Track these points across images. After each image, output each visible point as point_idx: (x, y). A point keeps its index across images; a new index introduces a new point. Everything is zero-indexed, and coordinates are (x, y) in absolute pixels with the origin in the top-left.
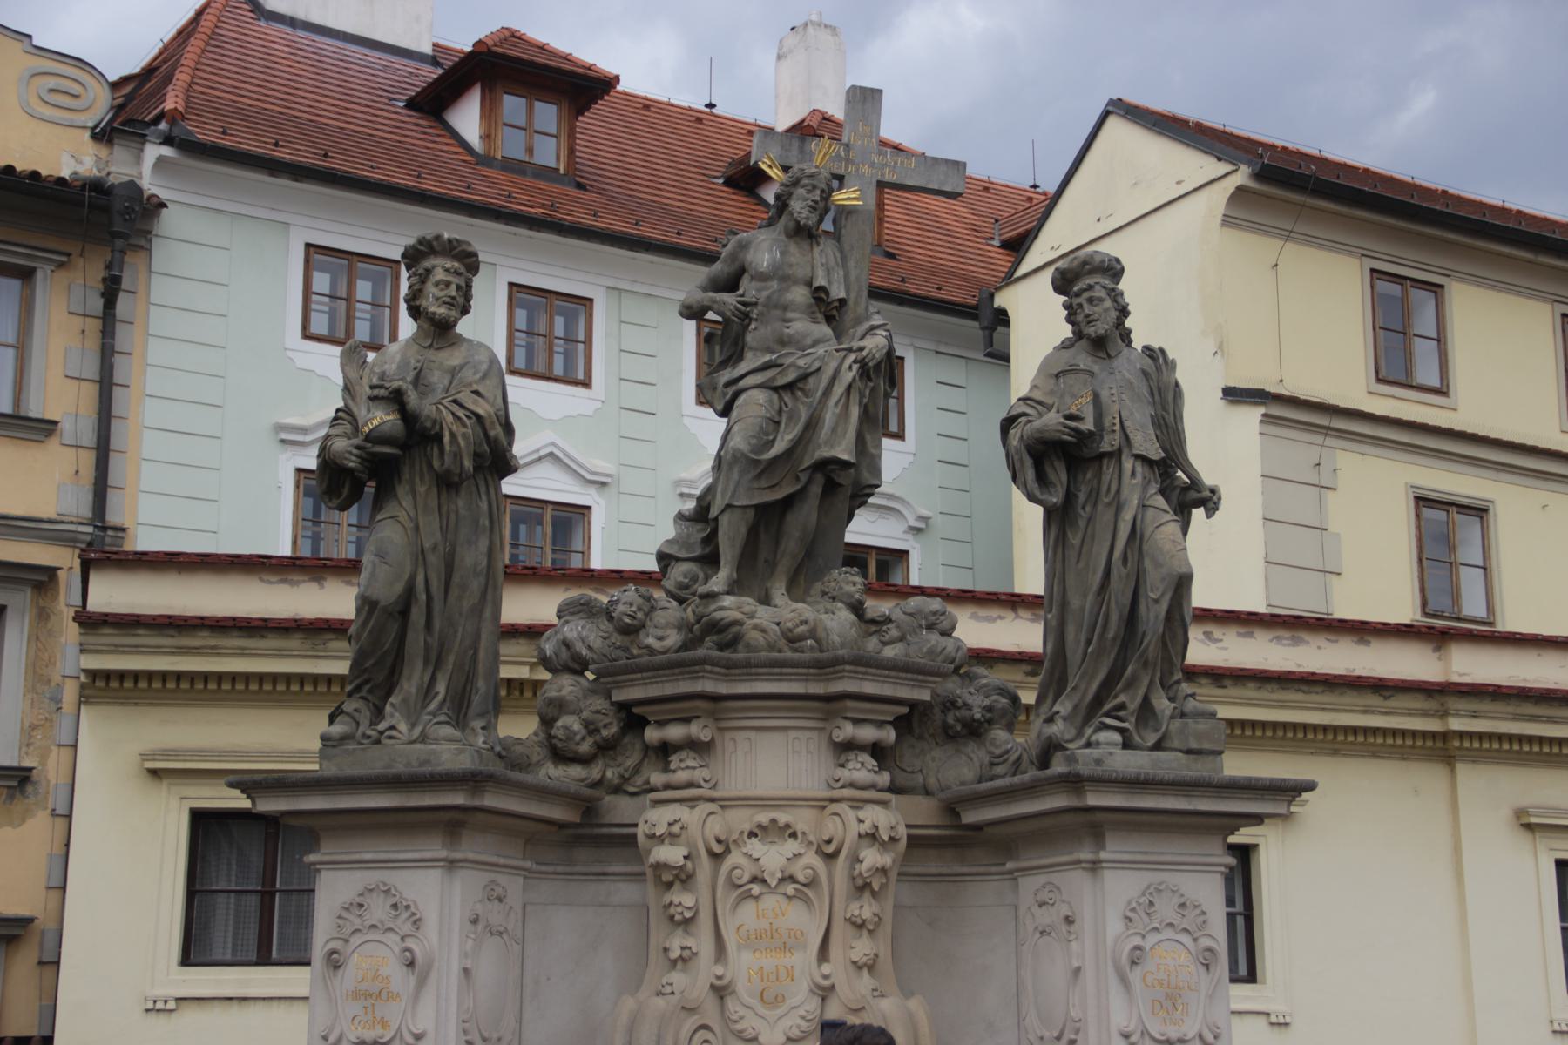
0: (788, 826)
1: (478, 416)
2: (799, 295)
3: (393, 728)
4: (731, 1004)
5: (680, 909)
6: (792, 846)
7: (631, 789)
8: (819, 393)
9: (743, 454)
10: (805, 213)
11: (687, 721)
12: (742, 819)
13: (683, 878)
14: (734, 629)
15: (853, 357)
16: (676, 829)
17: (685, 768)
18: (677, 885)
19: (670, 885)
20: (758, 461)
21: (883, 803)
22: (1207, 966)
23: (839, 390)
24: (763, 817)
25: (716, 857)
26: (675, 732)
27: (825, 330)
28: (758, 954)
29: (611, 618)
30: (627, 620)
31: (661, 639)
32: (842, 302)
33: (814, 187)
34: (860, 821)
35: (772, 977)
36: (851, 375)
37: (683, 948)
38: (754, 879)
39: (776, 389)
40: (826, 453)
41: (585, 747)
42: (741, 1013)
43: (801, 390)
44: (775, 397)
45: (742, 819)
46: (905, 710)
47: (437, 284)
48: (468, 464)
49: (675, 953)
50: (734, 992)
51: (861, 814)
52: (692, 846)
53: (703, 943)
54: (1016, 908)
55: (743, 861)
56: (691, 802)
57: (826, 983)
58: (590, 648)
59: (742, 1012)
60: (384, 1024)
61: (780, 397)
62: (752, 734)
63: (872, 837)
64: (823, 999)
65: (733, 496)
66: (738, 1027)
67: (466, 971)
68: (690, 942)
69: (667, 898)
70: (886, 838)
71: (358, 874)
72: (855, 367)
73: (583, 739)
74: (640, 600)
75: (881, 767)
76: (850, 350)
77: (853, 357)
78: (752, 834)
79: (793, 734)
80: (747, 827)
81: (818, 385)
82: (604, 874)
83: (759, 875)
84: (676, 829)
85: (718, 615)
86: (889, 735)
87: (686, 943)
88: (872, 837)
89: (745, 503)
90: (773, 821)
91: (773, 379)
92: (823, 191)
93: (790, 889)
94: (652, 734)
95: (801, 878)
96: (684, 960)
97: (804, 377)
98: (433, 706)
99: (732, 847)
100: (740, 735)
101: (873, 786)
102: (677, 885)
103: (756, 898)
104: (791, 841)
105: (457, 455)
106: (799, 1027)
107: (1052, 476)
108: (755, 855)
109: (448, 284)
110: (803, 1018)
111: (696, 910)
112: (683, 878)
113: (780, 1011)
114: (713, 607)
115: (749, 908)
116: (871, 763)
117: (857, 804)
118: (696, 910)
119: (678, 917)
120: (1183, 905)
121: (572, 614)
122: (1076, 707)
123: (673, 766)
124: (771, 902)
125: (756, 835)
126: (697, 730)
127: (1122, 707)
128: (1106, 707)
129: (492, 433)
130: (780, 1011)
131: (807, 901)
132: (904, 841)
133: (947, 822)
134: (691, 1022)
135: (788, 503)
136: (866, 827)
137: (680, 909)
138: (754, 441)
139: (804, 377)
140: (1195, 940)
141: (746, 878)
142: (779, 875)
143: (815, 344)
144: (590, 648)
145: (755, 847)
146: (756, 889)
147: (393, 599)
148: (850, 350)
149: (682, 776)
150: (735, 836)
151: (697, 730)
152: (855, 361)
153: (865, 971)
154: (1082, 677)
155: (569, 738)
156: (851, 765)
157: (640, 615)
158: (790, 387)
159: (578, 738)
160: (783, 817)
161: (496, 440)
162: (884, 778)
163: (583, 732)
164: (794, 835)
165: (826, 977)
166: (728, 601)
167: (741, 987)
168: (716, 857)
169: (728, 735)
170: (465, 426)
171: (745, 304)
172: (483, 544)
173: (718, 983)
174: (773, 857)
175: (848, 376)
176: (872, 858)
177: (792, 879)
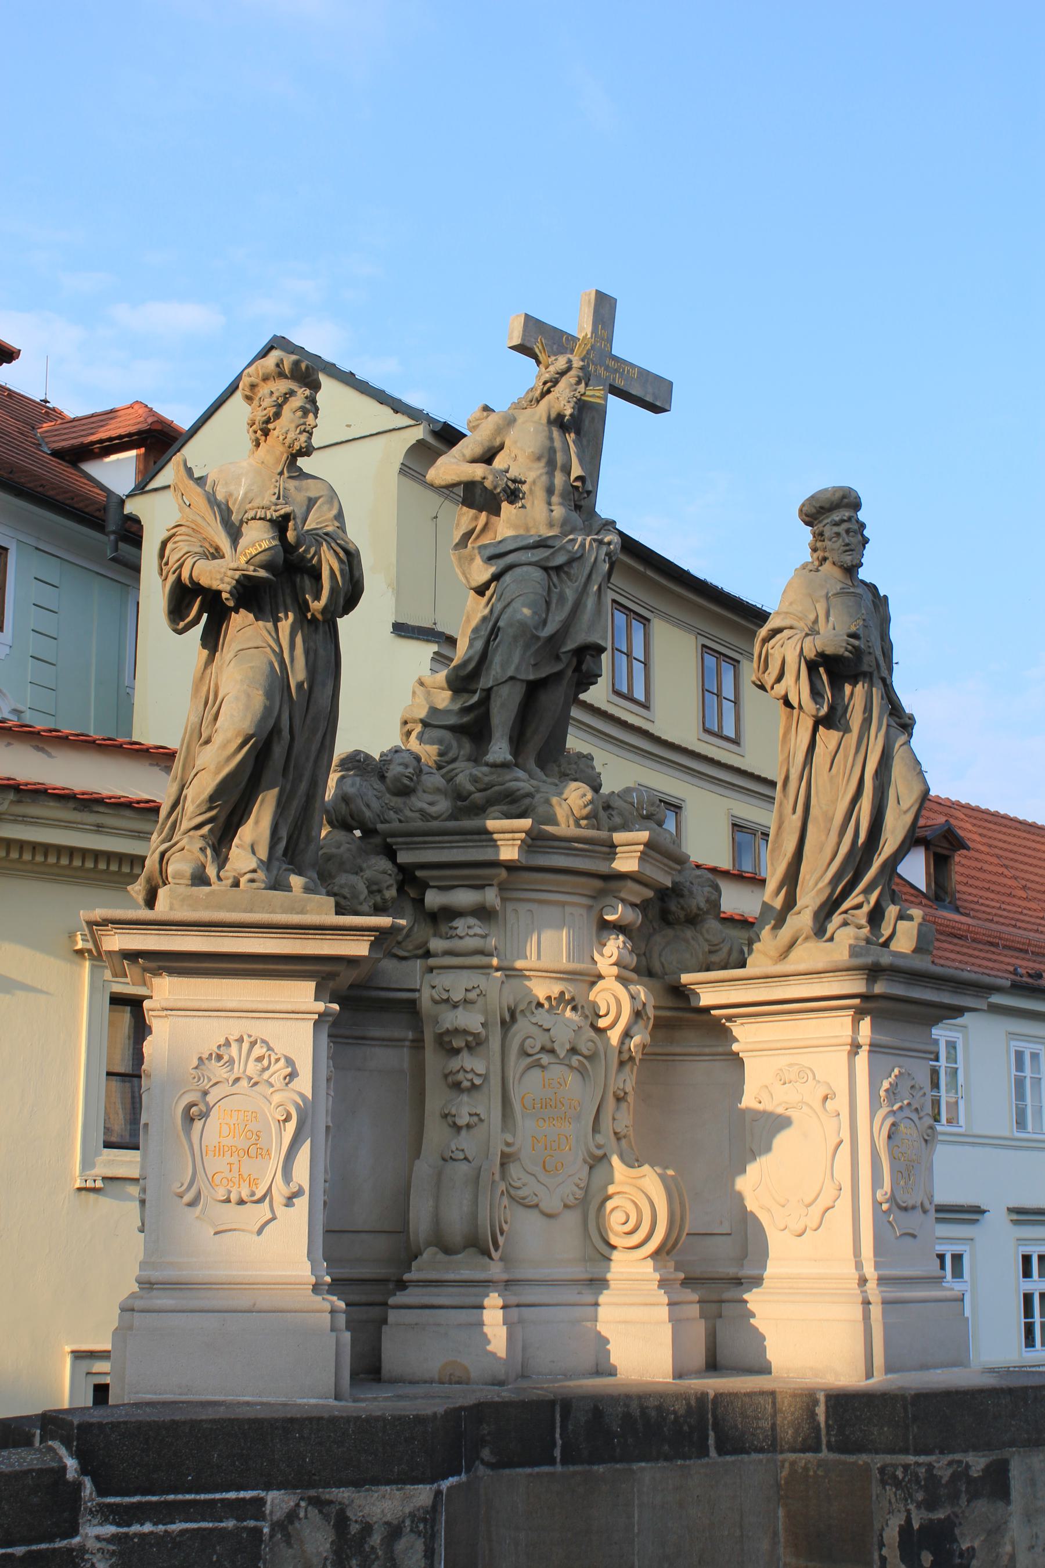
4: (514, 1170)
5: (470, 1076)
7: (401, 953)
11: (481, 887)
13: (475, 1043)
14: (527, 801)
16: (472, 995)
17: (468, 933)
18: (465, 1054)
19: (457, 1052)
22: (926, 1141)
29: (382, 777)
30: (406, 781)
31: (431, 804)
37: (470, 1115)
38: (543, 1049)
39: (546, 569)
43: (567, 573)
53: (489, 1106)
55: (534, 1031)
57: (599, 1153)
59: (526, 1178)
60: (253, 1182)
64: (591, 1168)
65: (517, 669)
66: (521, 1193)
69: (455, 1064)
71: (215, 1022)
81: (580, 572)
83: (549, 1045)
85: (514, 785)
91: (547, 559)
93: (575, 1060)
99: (518, 1016)
100: (523, 908)
102: (465, 1054)
103: (543, 1067)
108: (546, 1026)
110: (577, 1186)
111: (485, 1077)
112: (475, 1043)
114: (508, 777)
118: (485, 1077)
120: (912, 1087)
124: (557, 1071)
126: (491, 897)
127: (859, 906)
128: (845, 906)
131: (582, 1071)
133: (670, 1005)
137: (470, 1076)
140: (920, 1118)
141: (538, 1048)
146: (545, 1059)
149: (470, 943)
150: (521, 1007)
151: (491, 897)
158: (558, 569)
159: (362, 897)
165: (599, 1147)
169: (510, 906)
173: (507, 1150)
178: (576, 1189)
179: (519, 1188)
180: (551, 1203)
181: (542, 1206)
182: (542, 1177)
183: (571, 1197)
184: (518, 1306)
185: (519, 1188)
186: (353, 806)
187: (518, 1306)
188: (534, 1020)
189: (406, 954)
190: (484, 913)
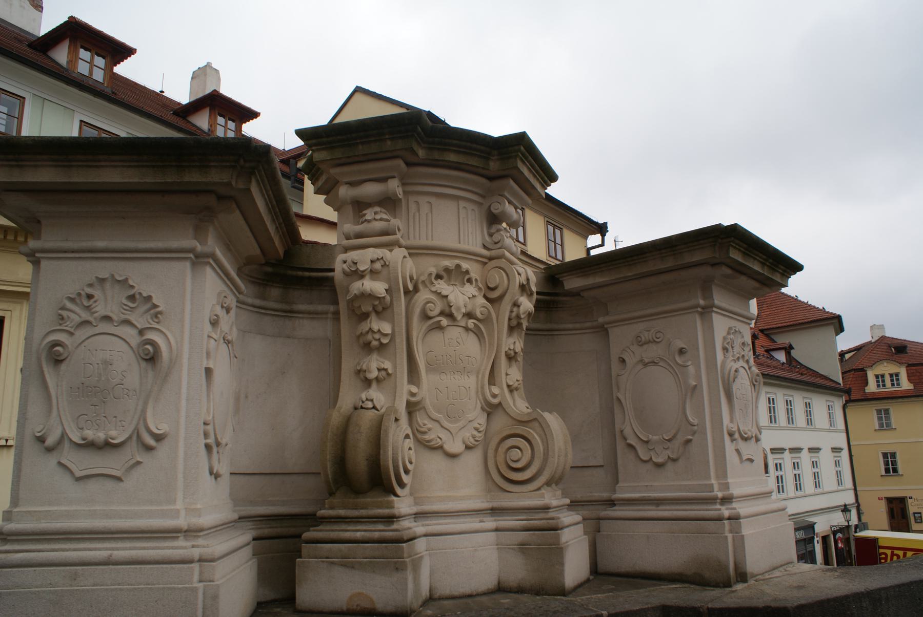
0: (467, 272)
4: (420, 418)
5: (377, 336)
6: (470, 290)
11: (384, 180)
12: (431, 265)
13: (382, 308)
16: (378, 266)
18: (373, 316)
19: (365, 316)
24: (449, 263)
37: (379, 370)
38: (442, 313)
42: (429, 426)
45: (431, 265)
49: (374, 374)
55: (433, 297)
56: (389, 246)
57: (495, 401)
59: (430, 424)
62: (433, 200)
64: (489, 414)
66: (427, 437)
68: (387, 365)
69: (364, 327)
78: (439, 277)
79: (462, 204)
80: (434, 271)
82: (291, 312)
83: (447, 310)
84: (378, 266)
90: (458, 266)
93: (471, 323)
95: (479, 315)
96: (384, 378)
99: (421, 287)
100: (423, 200)
102: (373, 316)
104: (468, 285)
108: (444, 293)
110: (476, 429)
111: (393, 336)
112: (382, 308)
113: (460, 424)
115: (436, 336)
118: (393, 336)
119: (375, 343)
124: (455, 333)
130: (460, 424)
141: (437, 311)
145: (442, 287)
146: (444, 322)
149: (378, 226)
150: (422, 278)
164: (469, 281)
165: (494, 396)
167: (428, 403)
169: (412, 199)
173: (413, 399)
178: (475, 433)
179: (425, 433)
180: (455, 446)
181: (446, 447)
182: (446, 424)
183: (472, 440)
184: (425, 535)
185: (425, 433)
187: (425, 535)
188: (433, 289)
190: (389, 203)
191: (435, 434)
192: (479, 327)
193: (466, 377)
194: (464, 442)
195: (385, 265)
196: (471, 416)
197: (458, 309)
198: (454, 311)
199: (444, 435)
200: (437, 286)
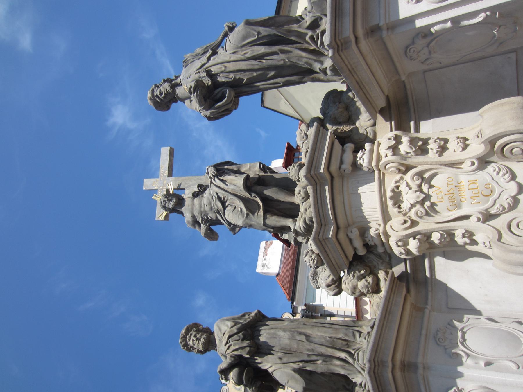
0: (393, 191)
1: (230, 337)
2: (196, 200)
3: (361, 384)
4: (493, 211)
6: (403, 188)
7: (388, 259)
8: (224, 192)
9: (245, 221)
10: (172, 203)
12: (392, 210)
14: (307, 221)
15: (212, 180)
20: (247, 215)
21: (379, 144)
23: (222, 185)
24: (390, 203)
25: (414, 223)
26: (358, 244)
27: (207, 192)
28: (463, 200)
30: (315, 262)
32: (200, 186)
33: (164, 201)
34: (386, 156)
35: (475, 191)
36: (218, 181)
39: (224, 208)
40: (242, 187)
41: (370, 279)
43: (224, 198)
44: (227, 209)
46: (337, 142)
47: (194, 345)
48: (246, 343)
50: (486, 210)
51: (383, 155)
52: (408, 236)
54: (425, 72)
55: (413, 210)
56: (387, 236)
58: (329, 276)
59: (497, 205)
61: (227, 206)
63: (395, 149)
66: (506, 206)
67: (488, 364)
70: (394, 142)
72: (216, 179)
73: (366, 281)
74: (308, 256)
75: (362, 147)
76: (211, 182)
77: (212, 180)
78: (399, 207)
80: (396, 210)
81: (222, 194)
86: (349, 147)
87: (461, 235)
88: (395, 149)
89: (262, 219)
90: (391, 198)
92: (166, 198)
93: (425, 188)
94: (362, 252)
95: (418, 182)
96: (469, 234)
97: (219, 198)
98: (350, 360)
101: (371, 151)
104: (400, 188)
105: (242, 348)
106: (504, 175)
107: (220, 95)
108: (409, 206)
109: (193, 341)
110: (498, 173)
114: (300, 231)
116: (360, 154)
117: (379, 158)
121: (317, 283)
122: (316, 61)
123: (373, 244)
125: (400, 205)
129: (235, 331)
132: (398, 133)
134: (507, 237)
135: (266, 200)
136: (390, 152)
138: (240, 216)
139: (219, 198)
142: (418, 193)
143: (210, 194)
144: (329, 276)
145: (405, 206)
147: (303, 381)
148: (211, 182)
152: (214, 179)
153: (467, 142)
154: (301, 61)
155: (367, 287)
156: (362, 163)
157: (313, 257)
158: (223, 203)
159: (366, 283)
160: (389, 194)
161: (238, 329)
162: (367, 146)
163: (363, 280)
164: (398, 187)
165: (473, 164)
166: (297, 225)
167: (482, 207)
168: (414, 223)
170: (231, 345)
171: (202, 221)
172: (281, 333)
174: (409, 197)
175: (218, 182)
176: (404, 147)
177: (420, 186)
178: (501, 173)
181: (513, 194)
186: (331, 284)
188: (408, 211)
189: (388, 256)
191: (505, 201)
192: (425, 179)
193: (461, 184)
194: (509, 182)
195: (400, 240)
196: (489, 179)
197: (418, 197)
198: (420, 199)
199: (504, 196)
200: (405, 209)
